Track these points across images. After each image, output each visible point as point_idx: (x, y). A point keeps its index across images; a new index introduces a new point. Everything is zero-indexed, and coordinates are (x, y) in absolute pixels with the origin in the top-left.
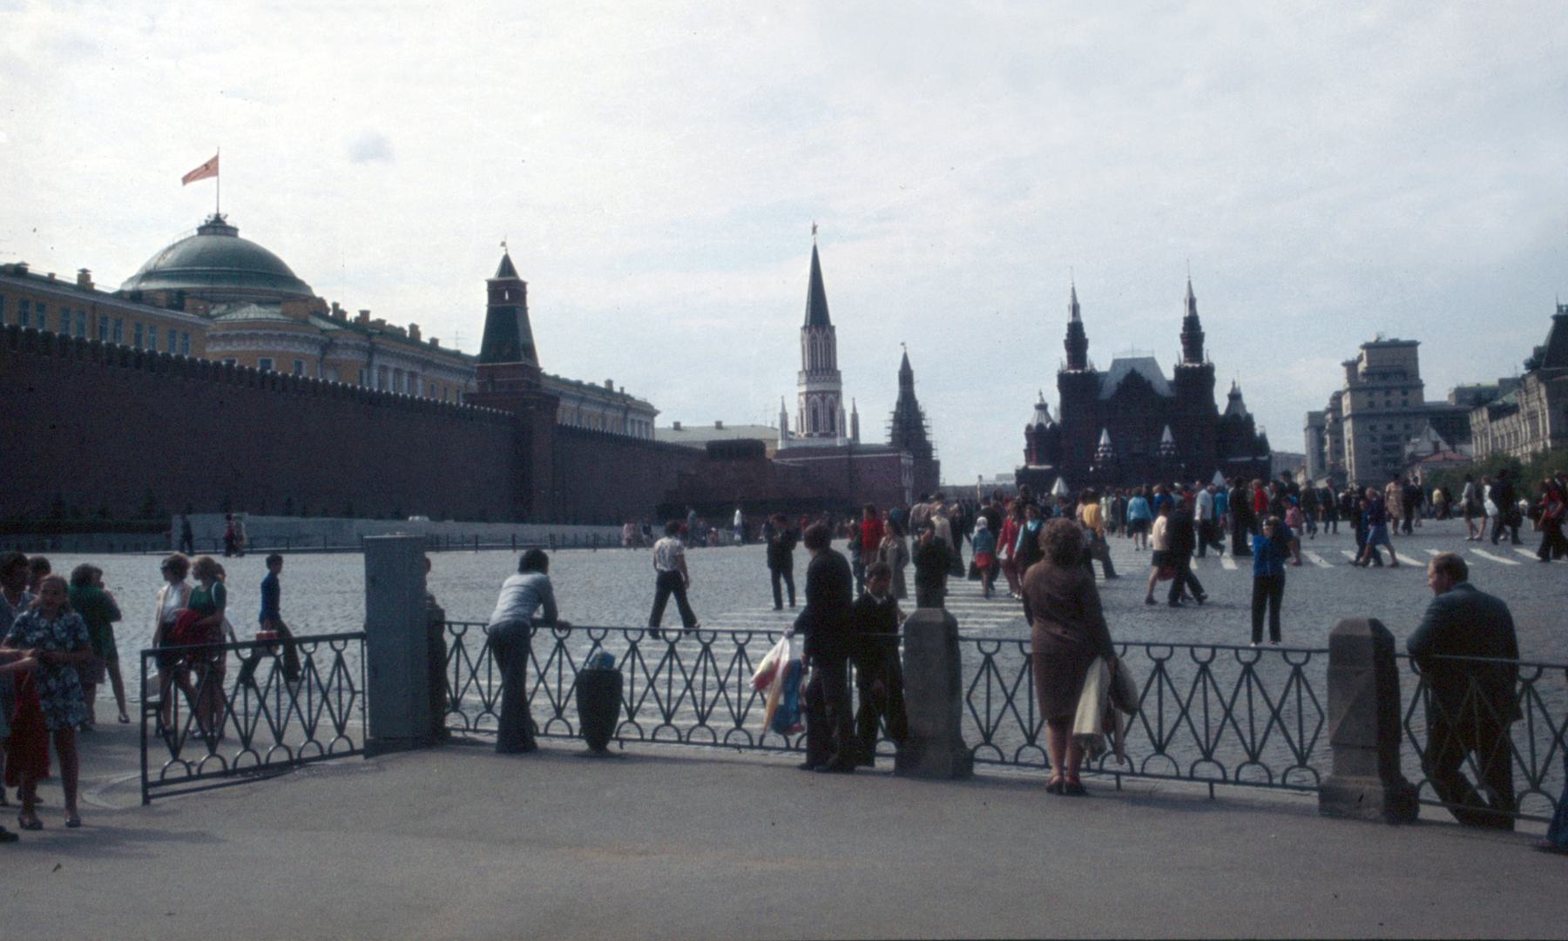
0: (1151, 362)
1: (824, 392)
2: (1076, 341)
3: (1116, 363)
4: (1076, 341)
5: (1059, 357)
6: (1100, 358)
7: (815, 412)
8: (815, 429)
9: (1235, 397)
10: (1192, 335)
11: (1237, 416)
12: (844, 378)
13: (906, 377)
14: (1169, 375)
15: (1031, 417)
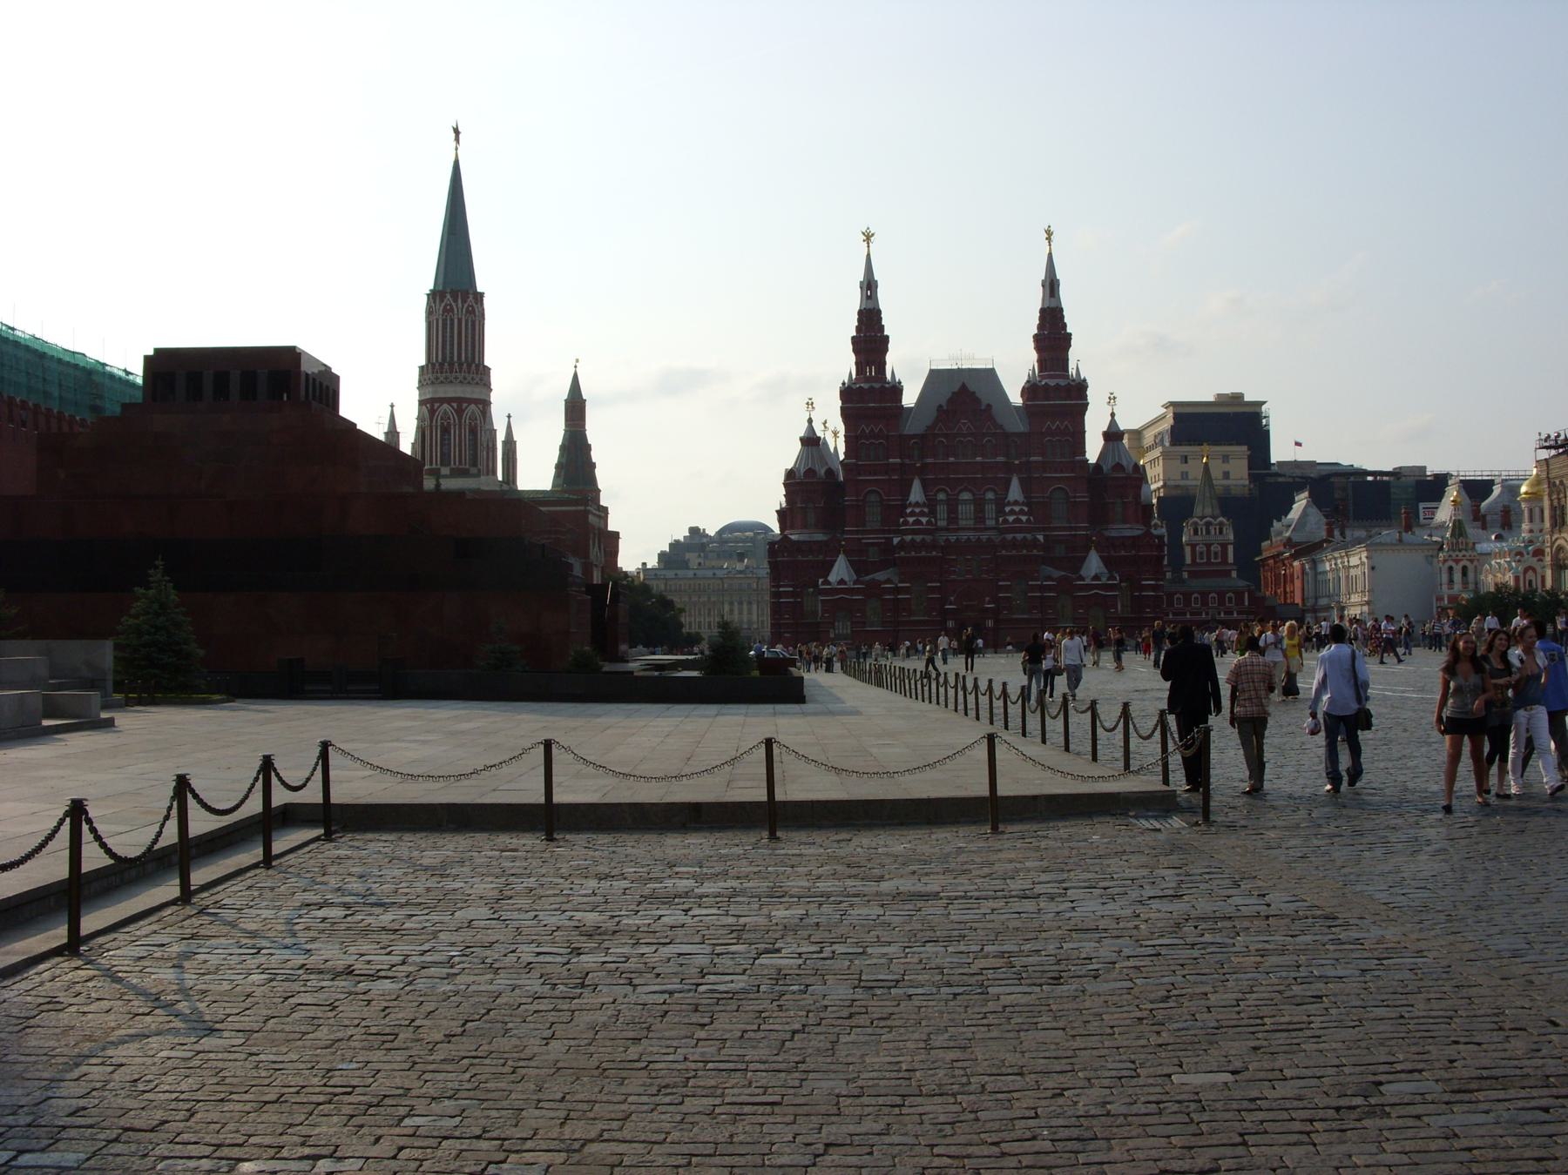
0: (989, 375)
1: (460, 400)
2: (870, 339)
3: (935, 377)
4: (870, 339)
5: (844, 365)
6: (909, 369)
7: (445, 430)
8: (445, 460)
9: (1113, 435)
10: (1052, 335)
11: (1118, 467)
12: (495, 380)
13: (575, 408)
14: (1016, 398)
15: (789, 455)
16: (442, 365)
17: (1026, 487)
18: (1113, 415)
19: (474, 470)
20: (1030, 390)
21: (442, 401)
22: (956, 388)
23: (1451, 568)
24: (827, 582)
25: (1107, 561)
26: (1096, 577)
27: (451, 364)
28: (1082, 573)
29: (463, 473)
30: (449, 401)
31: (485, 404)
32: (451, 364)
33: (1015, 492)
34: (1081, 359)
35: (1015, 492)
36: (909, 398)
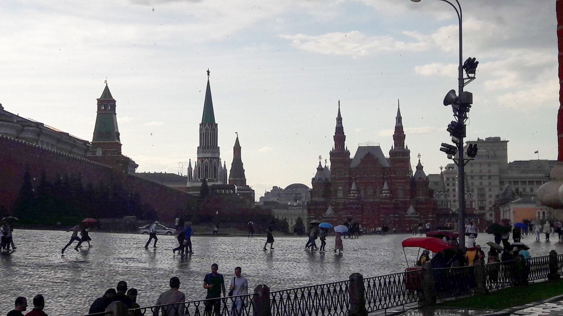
5: (331, 145)
6: (352, 147)
10: (399, 135)
14: (387, 155)
16: (205, 147)
17: (389, 184)
18: (419, 161)
19: (215, 180)
20: (391, 153)
21: (205, 158)
22: (367, 152)
23: (539, 212)
24: (325, 215)
25: (416, 209)
26: (412, 214)
27: (208, 147)
28: (408, 212)
29: (213, 181)
30: (208, 158)
31: (218, 159)
32: (208, 147)
33: (386, 187)
34: (408, 143)
35: (386, 187)
36: (352, 156)
